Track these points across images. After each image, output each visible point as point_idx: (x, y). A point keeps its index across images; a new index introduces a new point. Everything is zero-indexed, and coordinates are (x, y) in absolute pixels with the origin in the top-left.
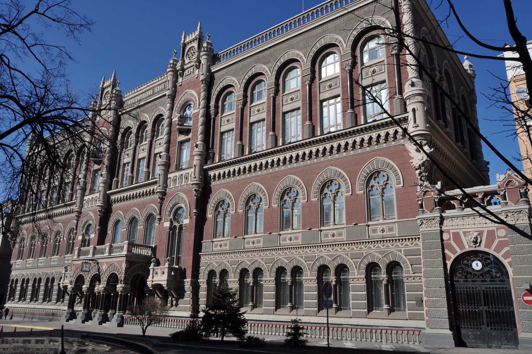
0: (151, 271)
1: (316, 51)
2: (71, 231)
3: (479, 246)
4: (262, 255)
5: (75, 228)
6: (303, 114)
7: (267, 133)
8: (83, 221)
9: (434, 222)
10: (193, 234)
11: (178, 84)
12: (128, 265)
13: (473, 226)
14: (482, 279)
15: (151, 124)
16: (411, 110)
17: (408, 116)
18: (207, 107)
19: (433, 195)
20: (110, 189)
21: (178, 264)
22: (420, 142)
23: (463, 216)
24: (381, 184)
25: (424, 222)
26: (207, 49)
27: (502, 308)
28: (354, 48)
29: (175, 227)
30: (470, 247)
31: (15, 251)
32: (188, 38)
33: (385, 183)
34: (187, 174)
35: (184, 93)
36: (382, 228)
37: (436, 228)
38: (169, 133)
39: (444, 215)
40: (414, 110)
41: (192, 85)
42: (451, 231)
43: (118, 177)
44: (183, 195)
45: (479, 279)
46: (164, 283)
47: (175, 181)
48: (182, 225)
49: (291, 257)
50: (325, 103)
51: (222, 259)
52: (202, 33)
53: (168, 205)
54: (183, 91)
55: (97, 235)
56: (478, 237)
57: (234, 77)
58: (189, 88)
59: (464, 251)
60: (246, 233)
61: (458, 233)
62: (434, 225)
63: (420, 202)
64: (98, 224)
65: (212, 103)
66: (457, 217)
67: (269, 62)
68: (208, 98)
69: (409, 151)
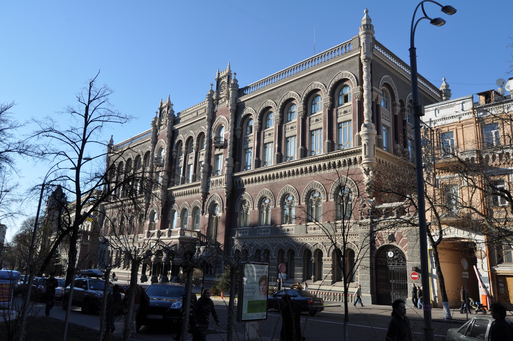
32: (221, 74)
40: (365, 145)
41: (224, 112)
47: (213, 184)
49: (287, 243)
52: (231, 71)
53: (208, 203)
55: (160, 221)
65: (238, 127)
68: (235, 123)
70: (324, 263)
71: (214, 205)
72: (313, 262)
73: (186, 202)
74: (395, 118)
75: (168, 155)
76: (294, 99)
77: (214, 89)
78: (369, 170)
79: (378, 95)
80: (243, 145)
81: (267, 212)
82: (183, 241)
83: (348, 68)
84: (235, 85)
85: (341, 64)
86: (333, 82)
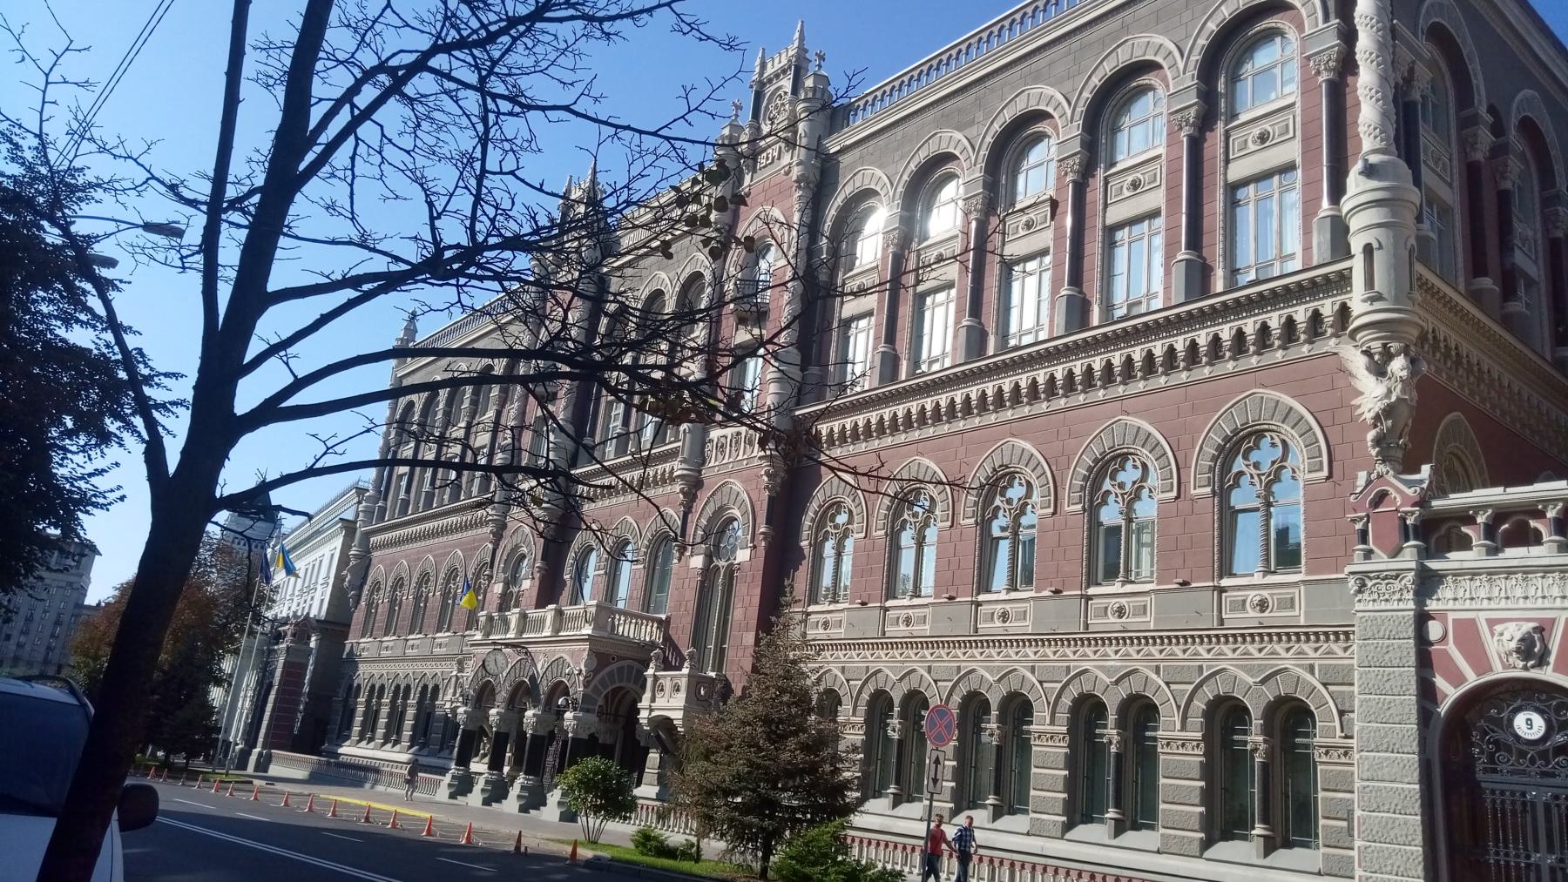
0: (650, 682)
1: (1099, 84)
2: (481, 567)
4: (961, 655)
5: (489, 560)
6: (1057, 265)
7: (957, 322)
8: (506, 543)
9: (1397, 585)
10: (758, 591)
13: (1521, 604)
15: (675, 298)
16: (1361, 249)
17: (1351, 269)
19: (1402, 505)
21: (718, 667)
22: (1384, 345)
23: (1491, 573)
24: (1265, 468)
25: (1370, 584)
26: (814, 94)
29: (717, 568)
30: (1506, 667)
31: (358, 616)
32: (769, 65)
33: (1276, 466)
36: (1258, 598)
37: (1402, 606)
39: (1434, 565)
40: (1368, 250)
42: (1451, 616)
45: (1532, 768)
46: (677, 716)
48: (732, 564)
50: (1122, 235)
51: (828, 662)
55: (537, 582)
57: (880, 167)
61: (1472, 622)
62: (1397, 596)
63: (1359, 526)
66: (1474, 574)
67: (972, 123)
68: (812, 228)
69: (1351, 374)
70: (1165, 757)
71: (719, 529)
72: (1113, 749)
73: (630, 519)
74: (1472, 173)
76: (1049, 116)
77: (746, 118)
78: (1388, 356)
79: (1414, 62)
81: (920, 542)
82: (602, 650)
86: (1212, 26)
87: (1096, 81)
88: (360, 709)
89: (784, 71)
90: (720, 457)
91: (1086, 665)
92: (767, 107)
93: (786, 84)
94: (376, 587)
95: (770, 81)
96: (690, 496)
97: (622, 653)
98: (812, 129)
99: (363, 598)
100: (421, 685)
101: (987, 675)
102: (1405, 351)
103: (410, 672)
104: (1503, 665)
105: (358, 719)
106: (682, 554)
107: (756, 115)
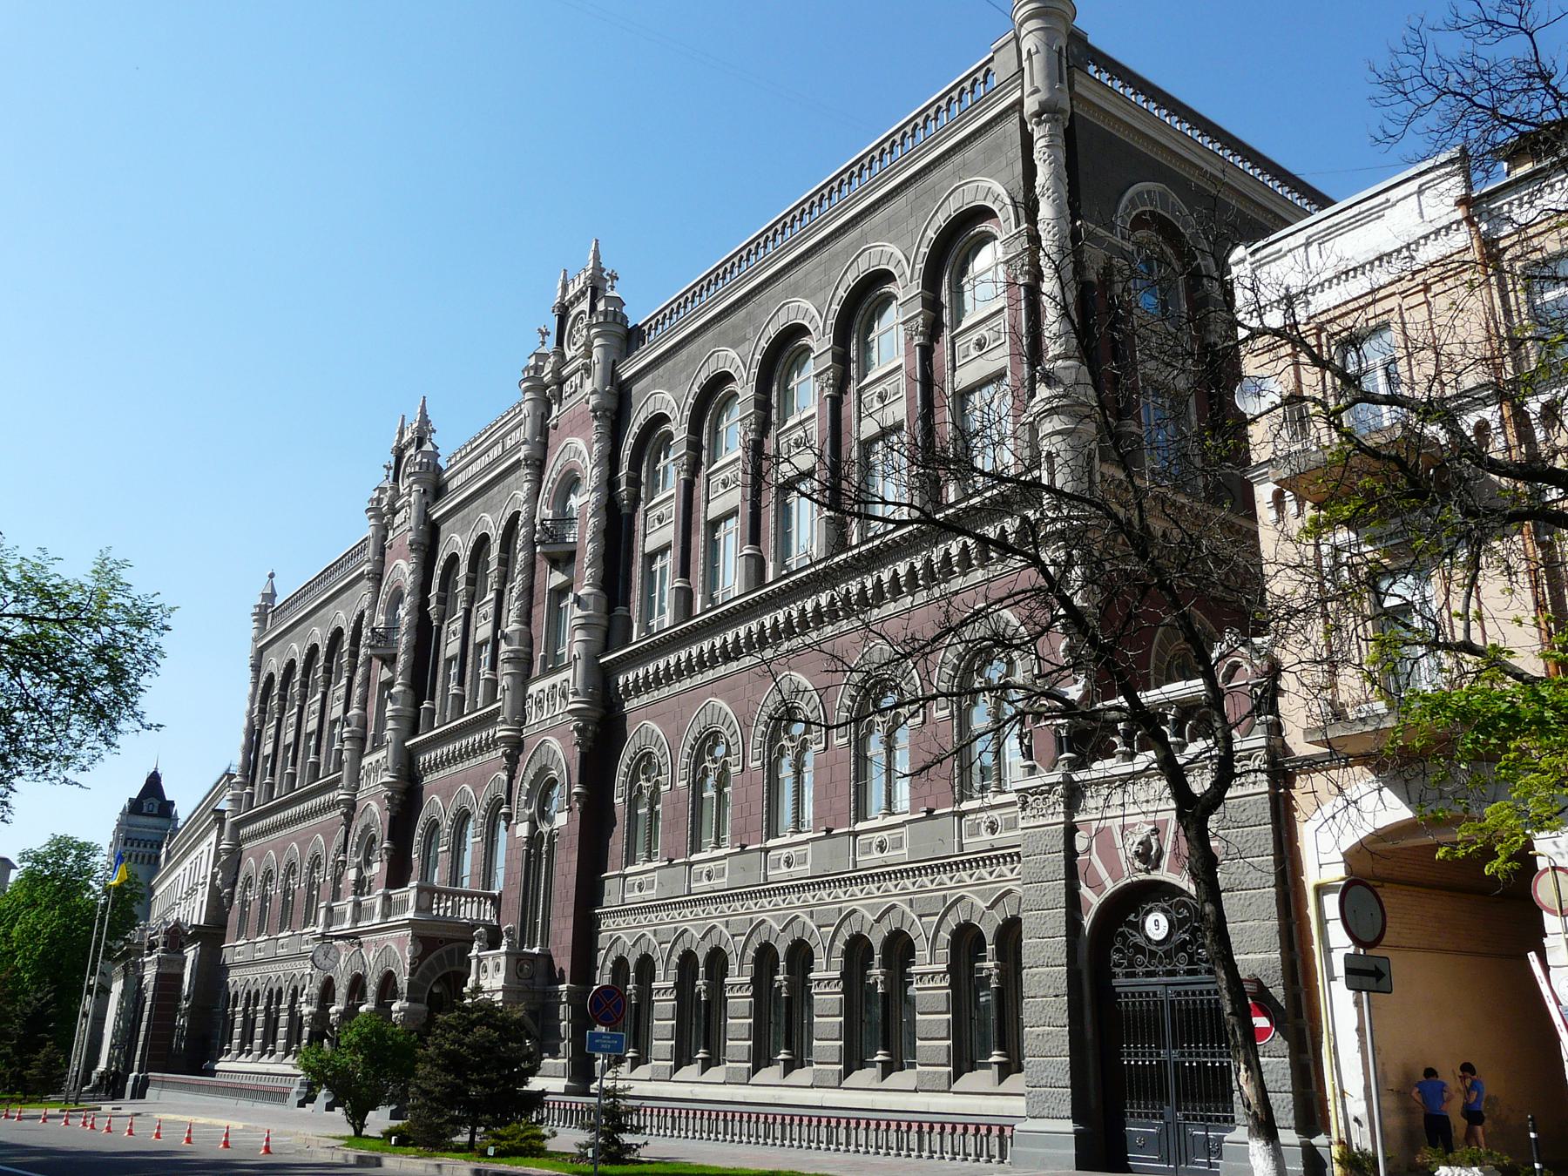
0: (474, 962)
3: (1157, 867)
8: (358, 825)
9: (1052, 798)
11: (552, 422)
12: (420, 948)
14: (1169, 967)
18: (611, 483)
20: (415, 733)
21: (545, 941)
25: (1030, 799)
26: (605, 318)
27: (1213, 1055)
28: (931, 279)
31: (233, 917)
32: (571, 287)
34: (565, 684)
35: (561, 448)
37: (1055, 820)
38: (531, 566)
39: (1078, 776)
43: (432, 698)
44: (555, 744)
47: (539, 703)
49: (785, 916)
54: (561, 441)
55: (386, 864)
56: (1153, 840)
57: (669, 390)
58: (571, 433)
59: (1121, 883)
60: (696, 847)
64: (386, 837)
67: (744, 339)
68: (611, 460)
73: (468, 788)
75: (416, 614)
80: (641, 538)
82: (427, 933)
83: (986, 166)
84: (616, 317)
85: (957, 159)
87: (842, 293)
88: (239, 1019)
89: (583, 293)
90: (552, 708)
91: (854, 905)
92: (570, 332)
93: (585, 305)
94: (248, 882)
95: (572, 304)
96: (513, 760)
97: (449, 934)
98: (606, 355)
99: (237, 897)
100: (292, 987)
101: (775, 925)
102: (1086, 560)
103: (281, 973)
104: (1134, 873)
105: (237, 1031)
106: (508, 823)
107: (560, 342)
